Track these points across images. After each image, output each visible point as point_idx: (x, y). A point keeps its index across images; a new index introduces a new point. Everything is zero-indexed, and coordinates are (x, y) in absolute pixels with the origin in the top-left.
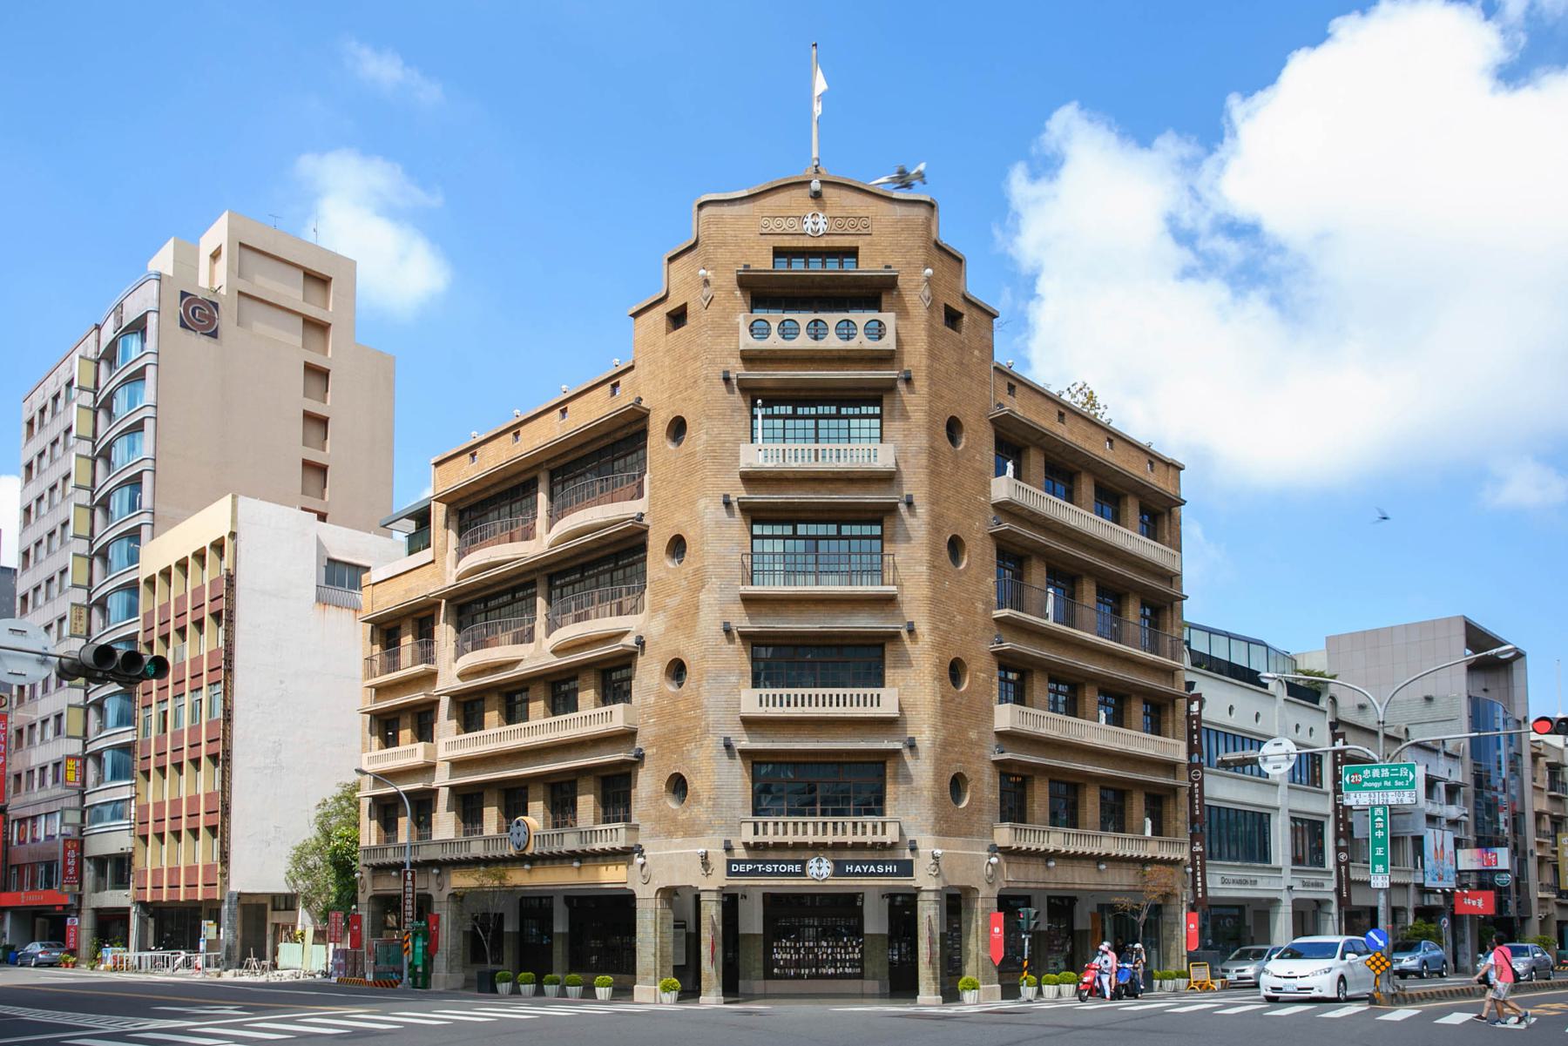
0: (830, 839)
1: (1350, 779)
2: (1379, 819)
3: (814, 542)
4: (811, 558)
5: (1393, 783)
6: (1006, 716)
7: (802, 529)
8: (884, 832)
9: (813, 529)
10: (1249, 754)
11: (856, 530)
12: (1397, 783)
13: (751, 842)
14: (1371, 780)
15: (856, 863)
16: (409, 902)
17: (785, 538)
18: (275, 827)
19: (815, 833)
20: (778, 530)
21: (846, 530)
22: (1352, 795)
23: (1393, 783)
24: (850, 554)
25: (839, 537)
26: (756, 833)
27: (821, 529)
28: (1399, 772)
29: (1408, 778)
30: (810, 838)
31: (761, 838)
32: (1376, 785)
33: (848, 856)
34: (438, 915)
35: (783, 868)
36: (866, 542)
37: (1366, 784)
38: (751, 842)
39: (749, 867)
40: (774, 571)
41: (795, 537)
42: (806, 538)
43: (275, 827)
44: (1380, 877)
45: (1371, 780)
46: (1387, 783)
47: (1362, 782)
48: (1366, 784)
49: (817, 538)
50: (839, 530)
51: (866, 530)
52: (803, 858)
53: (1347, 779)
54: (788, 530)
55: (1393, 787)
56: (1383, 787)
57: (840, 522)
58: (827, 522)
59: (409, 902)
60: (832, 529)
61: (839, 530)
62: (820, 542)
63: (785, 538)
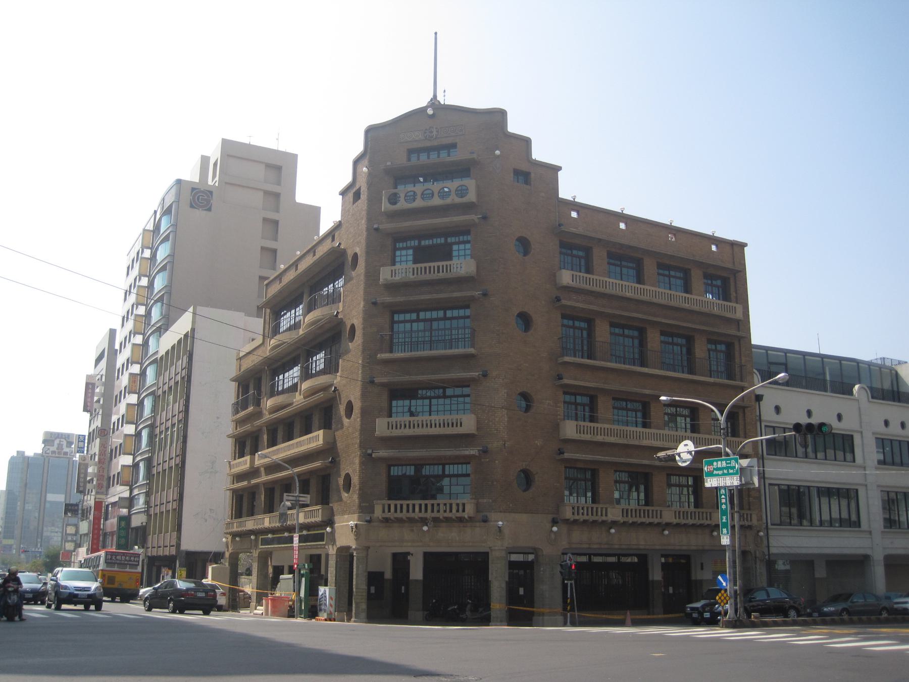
0: (429, 515)
1: (707, 469)
2: (723, 497)
3: (429, 323)
4: (427, 334)
5: (728, 471)
6: (570, 430)
7: (422, 315)
8: (464, 511)
9: (428, 315)
10: (670, 452)
11: (455, 313)
12: (731, 471)
14: (717, 469)
17: (412, 321)
18: (211, 510)
20: (408, 316)
21: (449, 314)
22: (709, 480)
23: (728, 471)
24: (451, 329)
25: (445, 318)
26: (384, 511)
27: (435, 314)
28: (730, 463)
29: (735, 467)
30: (417, 515)
31: (387, 515)
32: (720, 472)
36: (461, 321)
37: (715, 472)
38: (380, 517)
40: (458, 339)
41: (418, 320)
42: (425, 320)
43: (211, 510)
44: (725, 537)
45: (717, 469)
46: (725, 471)
47: (713, 471)
48: (715, 472)
49: (431, 320)
50: (445, 314)
51: (462, 312)
53: (706, 469)
54: (414, 316)
55: (729, 474)
56: (724, 474)
57: (445, 309)
58: (437, 309)
60: (441, 314)
61: (445, 314)
63: (412, 321)
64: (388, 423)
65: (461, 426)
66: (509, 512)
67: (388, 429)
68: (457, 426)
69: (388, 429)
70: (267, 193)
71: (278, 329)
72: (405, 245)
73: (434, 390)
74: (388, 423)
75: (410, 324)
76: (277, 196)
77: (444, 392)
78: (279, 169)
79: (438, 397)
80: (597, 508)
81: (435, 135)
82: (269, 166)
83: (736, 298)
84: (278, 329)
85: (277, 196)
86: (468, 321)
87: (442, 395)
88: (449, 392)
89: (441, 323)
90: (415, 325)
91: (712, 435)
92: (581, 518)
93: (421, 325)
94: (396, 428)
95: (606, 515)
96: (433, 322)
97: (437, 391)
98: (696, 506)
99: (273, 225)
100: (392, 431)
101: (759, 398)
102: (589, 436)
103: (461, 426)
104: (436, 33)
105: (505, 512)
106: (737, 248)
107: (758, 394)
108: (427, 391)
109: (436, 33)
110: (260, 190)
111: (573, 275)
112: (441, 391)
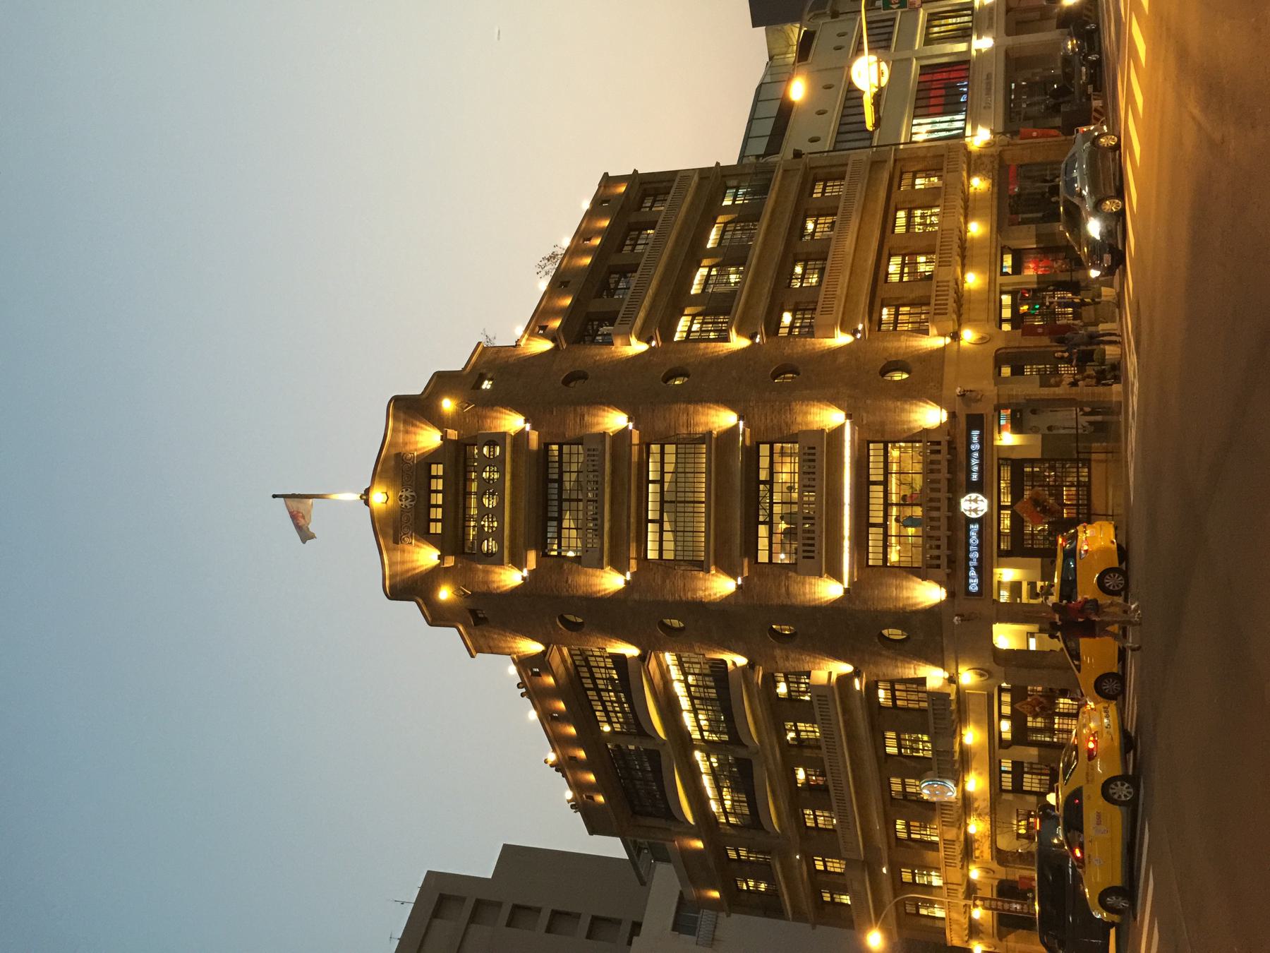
8: (939, 443)
13: (948, 571)
15: (969, 472)
16: (1006, 906)
17: (661, 531)
19: (938, 509)
26: (938, 566)
33: (962, 477)
34: (1020, 878)
35: (974, 541)
39: (973, 573)
41: (660, 522)
52: (964, 522)
59: (1006, 906)
62: (665, 499)
63: (661, 531)
64: (804, 557)
65: (814, 448)
66: (941, 385)
67: (813, 558)
68: (814, 454)
69: (813, 558)
70: (473, 918)
71: (644, 504)
72: (556, 503)
73: (760, 499)
74: (804, 557)
75: (664, 533)
76: (479, 903)
77: (764, 482)
78: (443, 900)
79: (771, 492)
80: (937, 291)
81: (413, 494)
82: (436, 914)
83: (669, 181)
84: (644, 504)
85: (479, 903)
86: (670, 449)
87: (768, 486)
88: (763, 475)
89: (666, 486)
90: (667, 526)
91: (845, 172)
92: (951, 305)
93: (666, 518)
94: (813, 545)
95: (948, 281)
96: (665, 499)
97: (762, 494)
98: (928, 304)
99: (520, 914)
100: (816, 552)
101: (798, 154)
102: (836, 302)
103: (814, 448)
104: (274, 496)
105: (942, 390)
106: (607, 181)
107: (792, 156)
108: (760, 507)
109: (274, 496)
110: (467, 929)
111: (620, 324)
112: (762, 487)
